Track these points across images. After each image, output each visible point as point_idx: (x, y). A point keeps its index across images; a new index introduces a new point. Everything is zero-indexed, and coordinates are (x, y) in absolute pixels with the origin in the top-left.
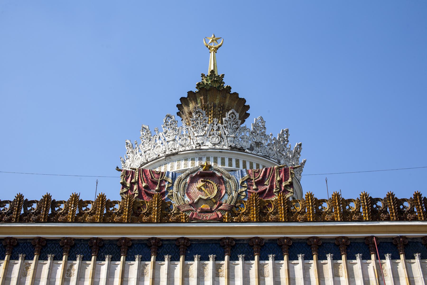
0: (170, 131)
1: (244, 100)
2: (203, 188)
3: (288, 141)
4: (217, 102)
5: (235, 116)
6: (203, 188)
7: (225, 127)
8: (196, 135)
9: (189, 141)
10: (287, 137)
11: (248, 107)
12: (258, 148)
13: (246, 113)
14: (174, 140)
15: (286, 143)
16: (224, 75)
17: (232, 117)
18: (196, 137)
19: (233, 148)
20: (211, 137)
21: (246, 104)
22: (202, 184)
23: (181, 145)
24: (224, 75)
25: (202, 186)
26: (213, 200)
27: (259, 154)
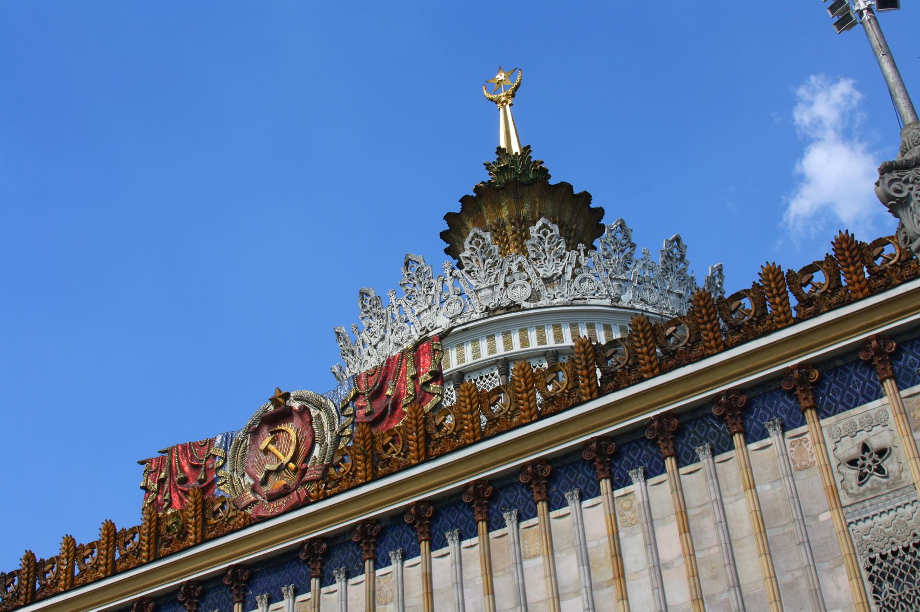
0: (374, 322)
1: (565, 188)
2: (272, 447)
3: (633, 246)
4: (505, 213)
5: (484, 240)
6: (272, 447)
7: (469, 272)
8: (416, 313)
9: (407, 331)
10: (627, 237)
11: (586, 197)
12: (550, 290)
13: (591, 209)
14: (383, 339)
15: (628, 250)
16: (529, 147)
17: (478, 244)
18: (418, 315)
19: (494, 311)
20: (445, 304)
21: (576, 191)
22: (269, 439)
23: (396, 344)
24: (529, 147)
25: (270, 443)
26: (292, 465)
27: (555, 302)
